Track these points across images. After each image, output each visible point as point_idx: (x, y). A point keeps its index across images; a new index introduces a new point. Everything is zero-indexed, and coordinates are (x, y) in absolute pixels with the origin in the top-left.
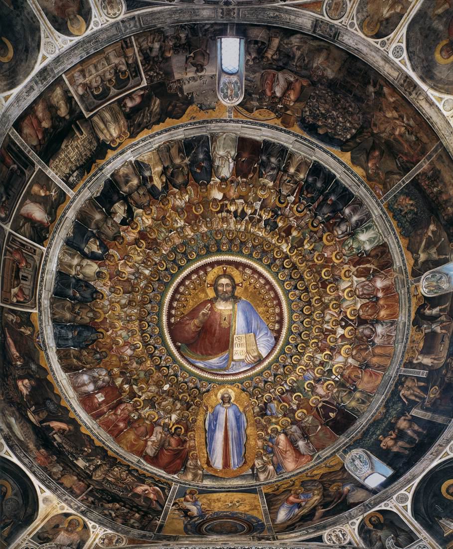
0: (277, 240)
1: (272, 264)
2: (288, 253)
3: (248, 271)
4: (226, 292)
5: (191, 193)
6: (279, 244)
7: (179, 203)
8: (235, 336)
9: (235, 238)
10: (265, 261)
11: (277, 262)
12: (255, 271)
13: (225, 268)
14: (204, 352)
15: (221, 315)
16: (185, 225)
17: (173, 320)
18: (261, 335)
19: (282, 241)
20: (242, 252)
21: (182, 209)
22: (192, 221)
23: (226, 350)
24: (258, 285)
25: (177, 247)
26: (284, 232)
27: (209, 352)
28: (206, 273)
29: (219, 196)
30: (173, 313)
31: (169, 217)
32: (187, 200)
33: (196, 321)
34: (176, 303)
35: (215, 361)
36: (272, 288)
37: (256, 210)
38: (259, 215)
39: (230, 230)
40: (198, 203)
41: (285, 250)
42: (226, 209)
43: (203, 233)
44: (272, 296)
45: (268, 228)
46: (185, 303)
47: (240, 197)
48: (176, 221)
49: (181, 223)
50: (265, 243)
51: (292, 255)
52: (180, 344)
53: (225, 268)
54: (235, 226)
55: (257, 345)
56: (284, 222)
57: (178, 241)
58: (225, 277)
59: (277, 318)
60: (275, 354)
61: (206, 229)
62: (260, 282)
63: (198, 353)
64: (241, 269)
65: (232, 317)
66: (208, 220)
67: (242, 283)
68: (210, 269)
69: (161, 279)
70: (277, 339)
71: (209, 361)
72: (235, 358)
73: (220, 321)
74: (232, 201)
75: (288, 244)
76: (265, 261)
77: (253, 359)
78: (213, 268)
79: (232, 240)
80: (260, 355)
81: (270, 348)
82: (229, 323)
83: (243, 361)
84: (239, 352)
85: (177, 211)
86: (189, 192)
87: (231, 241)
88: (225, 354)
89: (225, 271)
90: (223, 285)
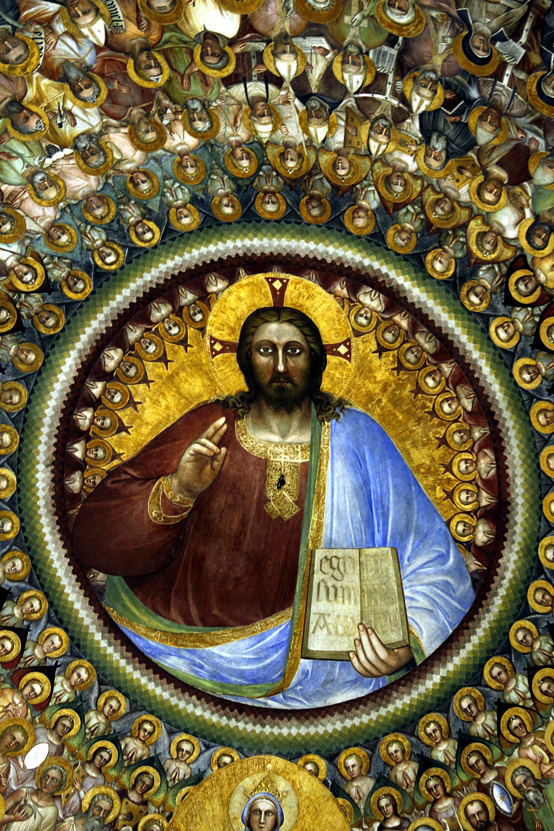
0: (479, 193)
1: (463, 280)
2: (524, 242)
3: (371, 300)
4: (287, 375)
5: (114, 14)
6: (487, 208)
7: (65, 49)
8: (319, 554)
9: (310, 174)
10: (440, 265)
11: (485, 277)
12: (395, 300)
13: (277, 285)
14: (194, 612)
15: (263, 464)
16: (106, 127)
17: (75, 483)
18: (419, 561)
19: (499, 197)
20: (342, 224)
21: (86, 70)
22: (139, 109)
23: (283, 608)
24: (411, 357)
25: (86, 203)
26: (500, 164)
27: (216, 612)
28: (205, 299)
29: (228, 24)
30: (79, 454)
31: (38, 101)
32: (101, 39)
33: (169, 487)
34: (88, 414)
35: (236, 652)
36: (466, 375)
37: (380, 77)
38: (394, 94)
39: (287, 145)
40: (147, 48)
41: (511, 234)
42: (263, 70)
43: (181, 155)
44: (468, 405)
45: (439, 145)
46: (125, 416)
47: (312, 29)
48: (69, 112)
49: (88, 120)
50: (430, 197)
51: (539, 254)
52: (101, 576)
53: (277, 285)
54: (306, 131)
55: (402, 597)
56: (498, 126)
57: (80, 183)
58: (278, 320)
59: (485, 499)
60: (469, 647)
61: (191, 141)
62: (419, 345)
63: (174, 613)
64: (341, 289)
65: (308, 474)
66: (197, 105)
67: (347, 343)
68: (221, 284)
69: (27, 323)
70: (483, 584)
71: (215, 650)
72: (318, 643)
73: (262, 490)
74: (282, 43)
75: (521, 209)
76: (440, 265)
77: (383, 654)
78: (231, 284)
79: (294, 180)
80: (409, 644)
81: (457, 620)
82: (300, 502)
83: (342, 658)
84: (335, 620)
85: (65, 79)
86: (104, 10)
87: (296, 188)
88: (275, 629)
89: (279, 296)
90: (274, 346)
